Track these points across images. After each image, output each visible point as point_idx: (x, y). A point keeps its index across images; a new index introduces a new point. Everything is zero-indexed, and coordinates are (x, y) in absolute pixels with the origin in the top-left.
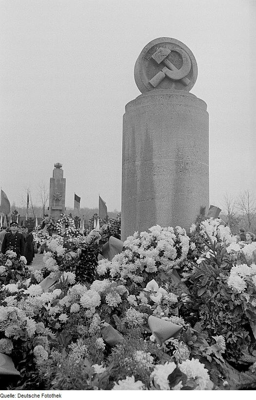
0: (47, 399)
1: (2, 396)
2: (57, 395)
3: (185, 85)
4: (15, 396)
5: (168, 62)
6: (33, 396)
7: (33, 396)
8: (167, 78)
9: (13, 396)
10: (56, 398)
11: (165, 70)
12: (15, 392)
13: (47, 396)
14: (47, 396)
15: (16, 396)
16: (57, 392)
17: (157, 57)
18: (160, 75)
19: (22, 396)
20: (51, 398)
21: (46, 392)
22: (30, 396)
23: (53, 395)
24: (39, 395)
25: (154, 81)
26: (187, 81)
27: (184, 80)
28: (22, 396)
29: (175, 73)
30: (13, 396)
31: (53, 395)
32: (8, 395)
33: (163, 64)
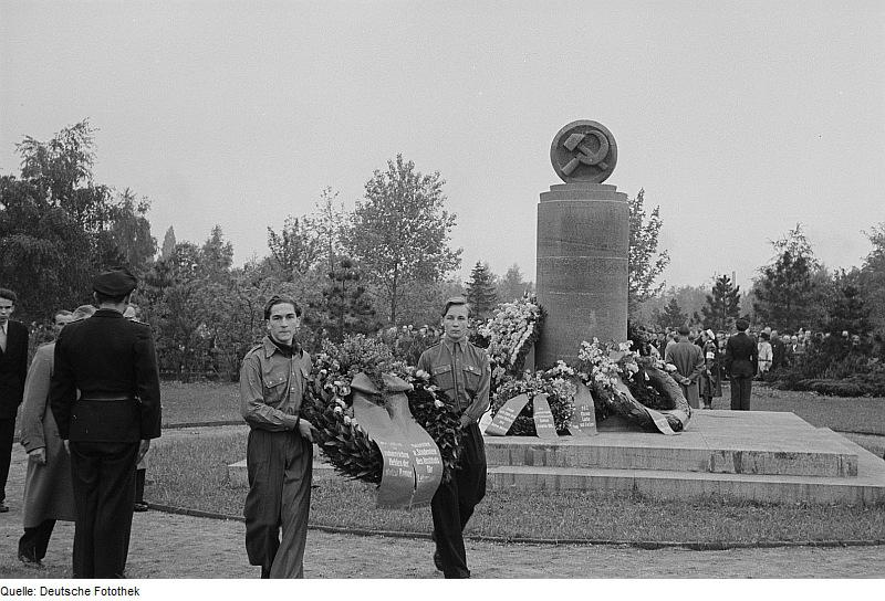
1: (5, 591)
2: (131, 591)
5: (583, 148)
6: (75, 592)
7: (75, 592)
9: (29, 592)
11: (580, 156)
12: (34, 583)
13: (108, 592)
15: (37, 592)
18: (573, 162)
19: (51, 592)
22: (68, 592)
23: (120, 591)
26: (605, 166)
28: (51, 592)
29: (592, 157)
30: (29, 592)
31: (120, 591)
33: (577, 150)
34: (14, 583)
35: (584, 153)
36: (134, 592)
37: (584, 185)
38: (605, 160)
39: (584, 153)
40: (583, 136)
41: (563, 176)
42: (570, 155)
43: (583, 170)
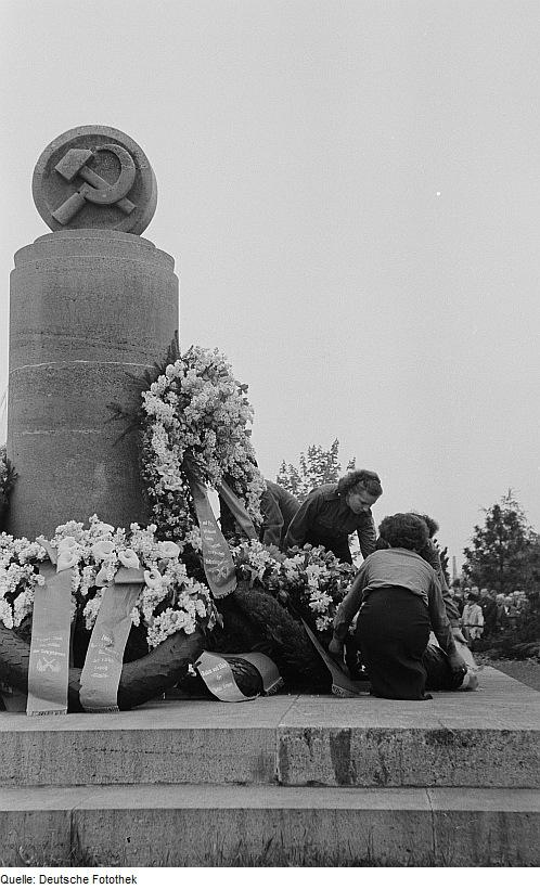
0: (105, 886)
1: (4, 879)
2: (128, 879)
3: (126, 214)
4: (34, 880)
5: (91, 175)
6: (73, 880)
7: (73, 880)
8: (87, 204)
9: (28, 880)
10: (125, 886)
11: (85, 188)
13: (105, 880)
14: (105, 880)
15: (37, 880)
16: (125, 872)
17: (65, 167)
18: (73, 200)
19: (50, 880)
20: (114, 886)
21: (102, 871)
23: (118, 879)
24: (86, 879)
25: (61, 212)
26: (129, 206)
27: (121, 204)
28: (50, 880)
29: (107, 189)
30: (28, 880)
31: (118, 879)
32: (19, 879)
33: (79, 179)
35: (95, 184)
37: (100, 240)
38: (129, 195)
39: (95, 184)
40: (89, 153)
41: (55, 224)
42: (70, 188)
43: (89, 213)
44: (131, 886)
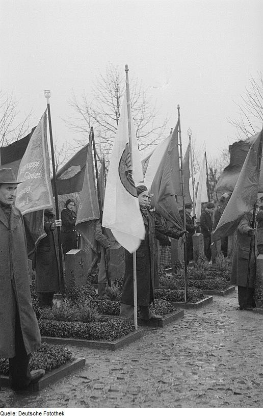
0: (49, 416)
1: (2, 413)
2: (60, 413)
4: (16, 414)
6: (34, 414)
7: (34, 414)
9: (13, 414)
12: (15, 410)
13: (49, 414)
14: (49, 414)
15: (17, 414)
16: (59, 410)
19: (23, 414)
20: (54, 416)
21: (48, 410)
22: (31, 414)
23: (56, 413)
24: (40, 413)
28: (23, 414)
30: (13, 414)
31: (56, 413)
32: (9, 413)
34: (6, 410)
36: (62, 414)
44: (62, 416)
